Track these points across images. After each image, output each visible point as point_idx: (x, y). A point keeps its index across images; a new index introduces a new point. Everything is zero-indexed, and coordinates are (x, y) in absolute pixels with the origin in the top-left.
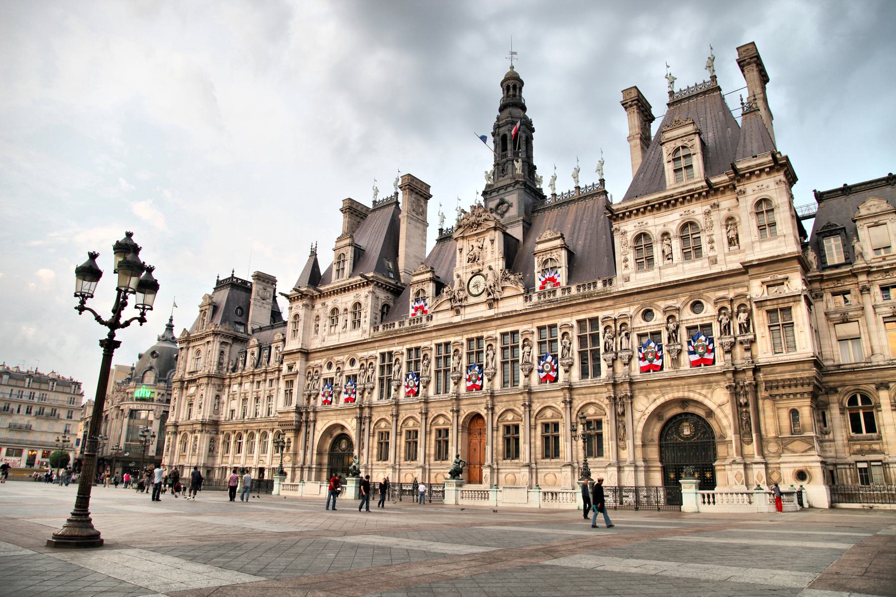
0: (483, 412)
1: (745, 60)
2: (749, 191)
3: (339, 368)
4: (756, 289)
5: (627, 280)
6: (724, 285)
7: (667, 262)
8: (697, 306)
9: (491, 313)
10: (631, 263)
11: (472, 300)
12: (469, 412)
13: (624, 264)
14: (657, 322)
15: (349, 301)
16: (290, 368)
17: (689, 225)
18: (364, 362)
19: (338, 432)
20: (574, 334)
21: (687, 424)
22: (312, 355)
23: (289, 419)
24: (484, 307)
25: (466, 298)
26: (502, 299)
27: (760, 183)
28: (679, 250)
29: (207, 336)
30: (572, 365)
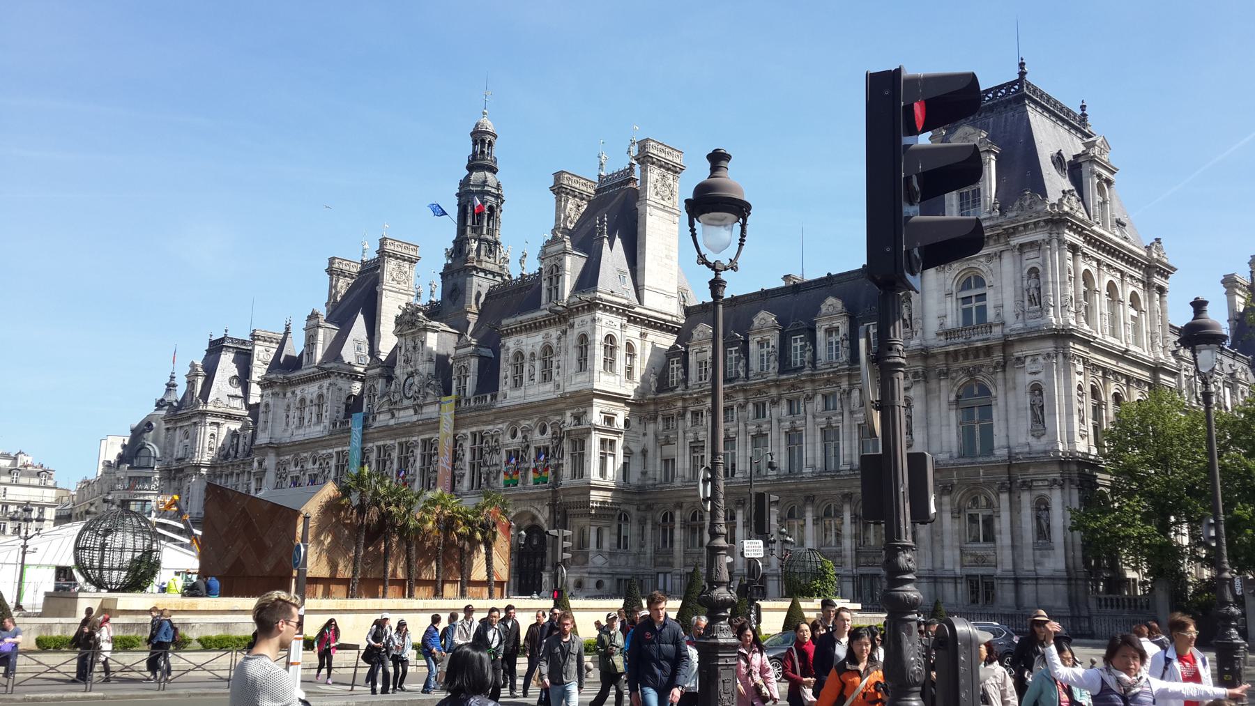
2: (576, 326)
3: (302, 467)
6: (560, 410)
8: (543, 432)
9: (415, 418)
10: (510, 381)
11: (406, 402)
16: (260, 464)
17: (548, 350)
18: (322, 461)
21: (535, 535)
22: (282, 449)
24: (412, 412)
25: (401, 400)
26: (425, 405)
29: (193, 416)
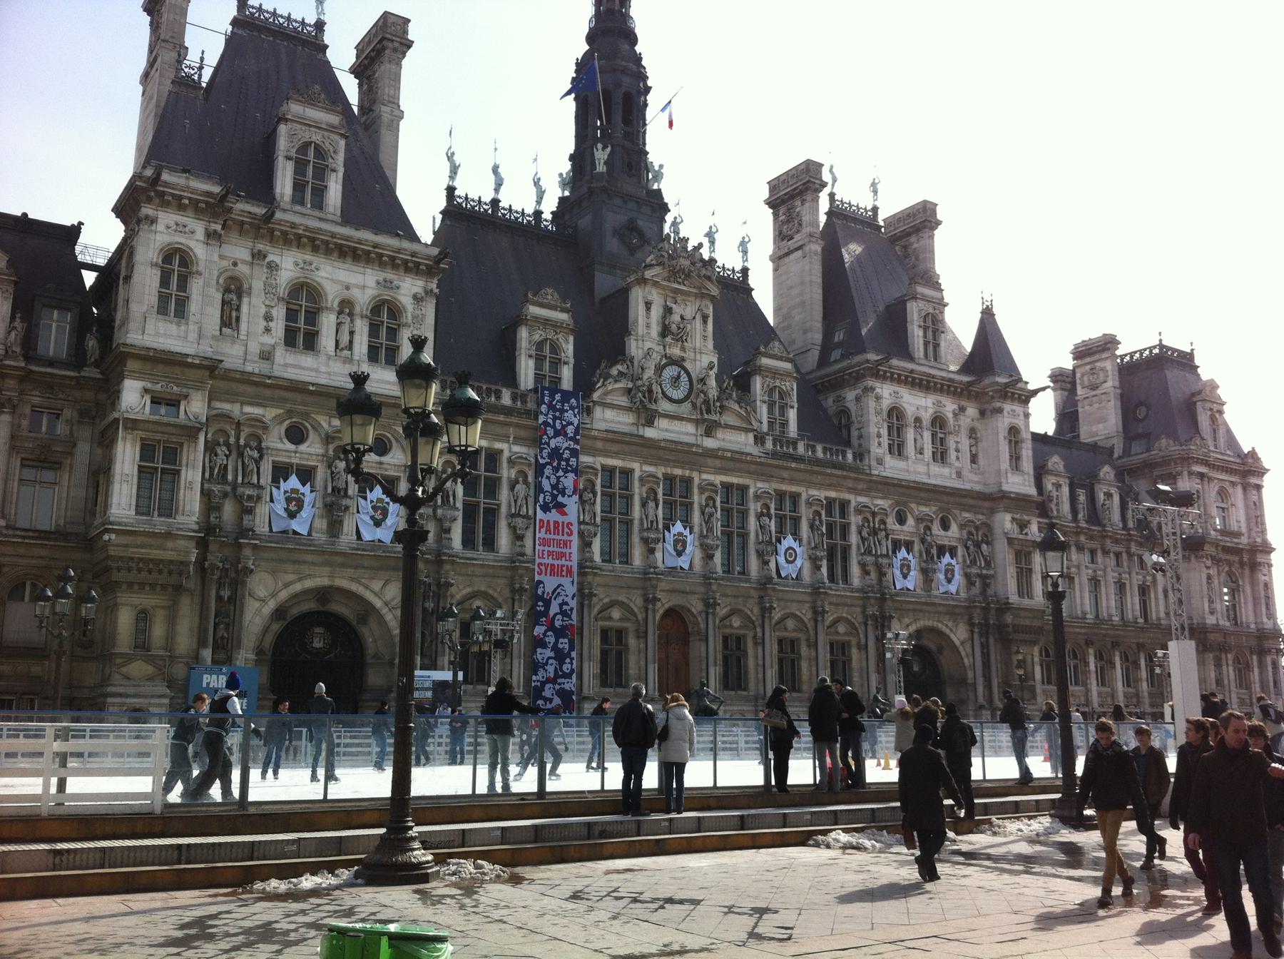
0: (696, 606)
1: (930, 222)
4: (1005, 522)
5: (880, 462)
7: (918, 456)
8: (945, 526)
9: (709, 443)
10: (885, 441)
12: (671, 604)
13: (877, 440)
14: (911, 530)
15: (364, 287)
17: (938, 422)
19: (310, 606)
20: (823, 513)
23: (170, 555)
24: (690, 428)
26: (727, 426)
27: (1014, 408)
28: (930, 446)
30: (821, 560)
